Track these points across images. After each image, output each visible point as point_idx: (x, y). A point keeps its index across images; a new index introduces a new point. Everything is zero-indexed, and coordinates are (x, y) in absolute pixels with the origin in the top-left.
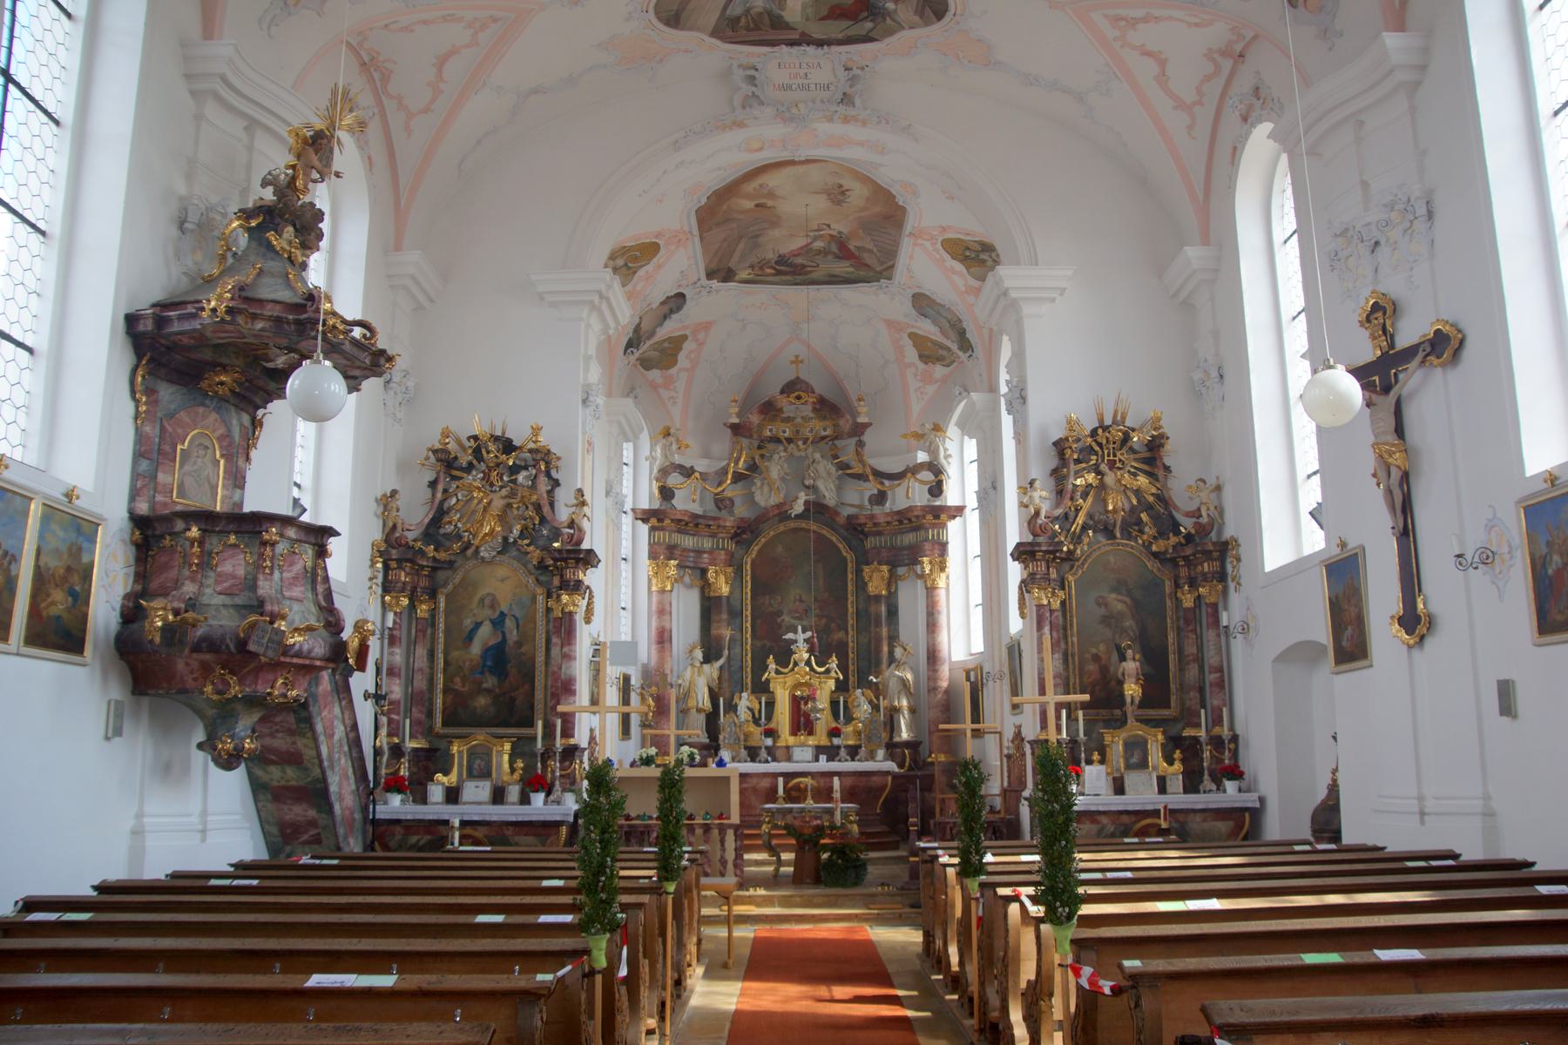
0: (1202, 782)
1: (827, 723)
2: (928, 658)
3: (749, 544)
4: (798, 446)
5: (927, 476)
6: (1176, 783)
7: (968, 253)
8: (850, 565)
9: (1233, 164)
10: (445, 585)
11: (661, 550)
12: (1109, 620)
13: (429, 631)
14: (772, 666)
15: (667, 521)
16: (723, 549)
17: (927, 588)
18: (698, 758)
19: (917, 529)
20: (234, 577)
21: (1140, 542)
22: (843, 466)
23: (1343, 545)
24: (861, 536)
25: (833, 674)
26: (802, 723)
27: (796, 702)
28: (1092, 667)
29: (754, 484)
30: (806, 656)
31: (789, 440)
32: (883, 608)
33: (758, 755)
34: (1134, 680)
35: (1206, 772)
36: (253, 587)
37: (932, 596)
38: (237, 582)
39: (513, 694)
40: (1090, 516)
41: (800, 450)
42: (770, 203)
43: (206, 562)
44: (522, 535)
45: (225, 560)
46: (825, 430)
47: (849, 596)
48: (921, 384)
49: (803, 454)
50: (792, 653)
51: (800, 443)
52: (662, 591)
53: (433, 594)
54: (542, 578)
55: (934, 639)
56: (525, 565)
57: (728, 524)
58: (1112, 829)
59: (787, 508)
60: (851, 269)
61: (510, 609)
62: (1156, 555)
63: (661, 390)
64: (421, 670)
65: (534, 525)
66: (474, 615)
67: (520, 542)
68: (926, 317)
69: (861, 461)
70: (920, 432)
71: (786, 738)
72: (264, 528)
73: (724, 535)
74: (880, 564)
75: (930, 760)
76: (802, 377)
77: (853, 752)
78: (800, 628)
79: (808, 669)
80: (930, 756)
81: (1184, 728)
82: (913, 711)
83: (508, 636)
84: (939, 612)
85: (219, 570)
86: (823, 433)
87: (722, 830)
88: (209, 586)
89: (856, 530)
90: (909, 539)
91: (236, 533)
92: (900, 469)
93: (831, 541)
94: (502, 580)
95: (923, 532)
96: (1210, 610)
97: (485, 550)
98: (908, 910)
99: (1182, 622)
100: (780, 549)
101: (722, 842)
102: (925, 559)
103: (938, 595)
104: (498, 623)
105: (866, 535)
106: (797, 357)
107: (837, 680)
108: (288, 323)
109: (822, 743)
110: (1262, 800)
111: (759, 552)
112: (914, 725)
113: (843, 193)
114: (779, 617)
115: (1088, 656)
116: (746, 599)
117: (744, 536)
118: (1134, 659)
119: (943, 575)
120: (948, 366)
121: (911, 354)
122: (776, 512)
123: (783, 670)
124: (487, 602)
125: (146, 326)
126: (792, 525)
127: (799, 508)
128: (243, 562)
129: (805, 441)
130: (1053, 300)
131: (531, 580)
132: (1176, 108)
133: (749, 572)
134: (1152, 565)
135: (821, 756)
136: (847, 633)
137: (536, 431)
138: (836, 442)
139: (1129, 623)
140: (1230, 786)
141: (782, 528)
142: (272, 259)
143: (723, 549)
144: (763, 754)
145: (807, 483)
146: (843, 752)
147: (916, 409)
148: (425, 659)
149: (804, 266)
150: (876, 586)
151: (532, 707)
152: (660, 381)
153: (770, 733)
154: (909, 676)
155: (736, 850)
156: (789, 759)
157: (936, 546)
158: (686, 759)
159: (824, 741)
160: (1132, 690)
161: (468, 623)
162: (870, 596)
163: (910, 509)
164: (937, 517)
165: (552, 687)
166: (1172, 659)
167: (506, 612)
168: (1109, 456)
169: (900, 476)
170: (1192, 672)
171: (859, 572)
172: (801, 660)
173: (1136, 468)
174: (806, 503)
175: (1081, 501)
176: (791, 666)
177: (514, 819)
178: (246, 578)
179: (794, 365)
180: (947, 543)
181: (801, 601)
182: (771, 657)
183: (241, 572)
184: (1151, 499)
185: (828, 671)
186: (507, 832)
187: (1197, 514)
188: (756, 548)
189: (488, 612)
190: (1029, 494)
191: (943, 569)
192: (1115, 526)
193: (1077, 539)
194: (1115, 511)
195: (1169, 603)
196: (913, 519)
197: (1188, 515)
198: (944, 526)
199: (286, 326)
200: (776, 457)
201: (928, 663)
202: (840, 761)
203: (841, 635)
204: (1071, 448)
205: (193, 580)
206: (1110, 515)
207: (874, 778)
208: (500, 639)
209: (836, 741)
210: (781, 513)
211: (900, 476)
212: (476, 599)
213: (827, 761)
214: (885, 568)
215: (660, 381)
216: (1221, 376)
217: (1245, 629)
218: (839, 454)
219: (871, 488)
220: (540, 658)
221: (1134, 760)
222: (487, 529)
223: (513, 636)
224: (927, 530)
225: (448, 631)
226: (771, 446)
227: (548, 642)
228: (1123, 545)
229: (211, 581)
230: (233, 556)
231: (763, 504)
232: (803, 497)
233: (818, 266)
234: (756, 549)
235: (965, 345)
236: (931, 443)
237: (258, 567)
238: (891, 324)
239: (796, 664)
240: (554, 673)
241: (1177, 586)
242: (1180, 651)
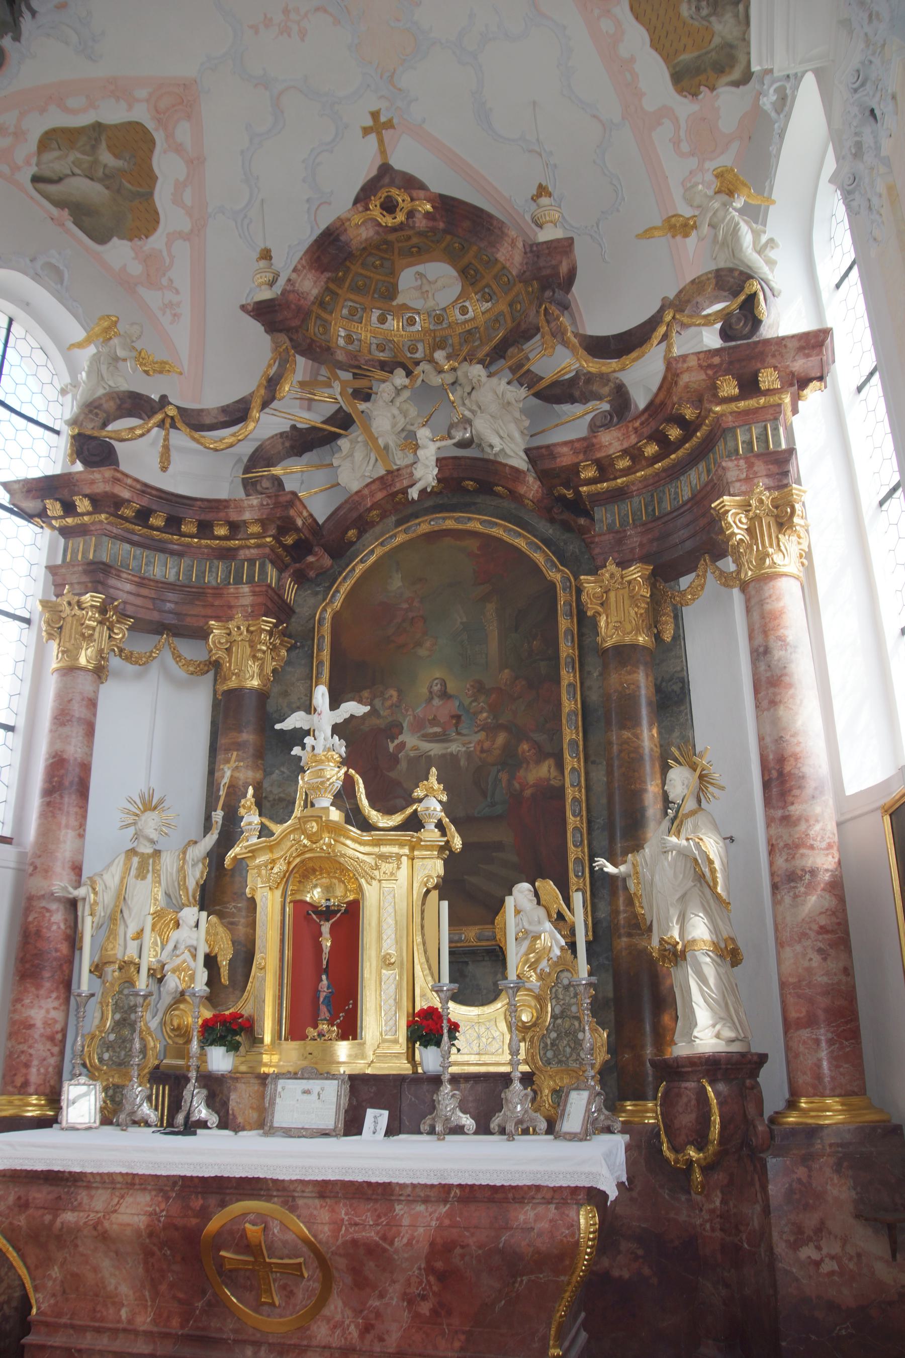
2: (766, 785)
3: (328, 579)
11: (76, 576)
15: (83, 505)
16: (250, 581)
37: (761, 603)
41: (440, 371)
48: (693, 162)
52: (70, 670)
55: (775, 721)
57: (247, 516)
63: (141, 290)
73: (254, 551)
74: (623, 564)
79: (335, 815)
80: (792, 1105)
100: (396, 583)
106: (375, 115)
117: (311, 559)
119: (789, 542)
122: (380, 496)
126: (424, 526)
135: (370, 1113)
143: (250, 581)
152: (136, 269)
154: (712, 846)
157: (760, 467)
179: (373, 138)
180: (791, 451)
181: (445, 695)
185: (414, 823)
188: (345, 587)
196: (689, 413)
201: (768, 802)
202: (432, 1131)
203: (544, 770)
207: (526, 1215)
213: (390, 1132)
215: (136, 269)
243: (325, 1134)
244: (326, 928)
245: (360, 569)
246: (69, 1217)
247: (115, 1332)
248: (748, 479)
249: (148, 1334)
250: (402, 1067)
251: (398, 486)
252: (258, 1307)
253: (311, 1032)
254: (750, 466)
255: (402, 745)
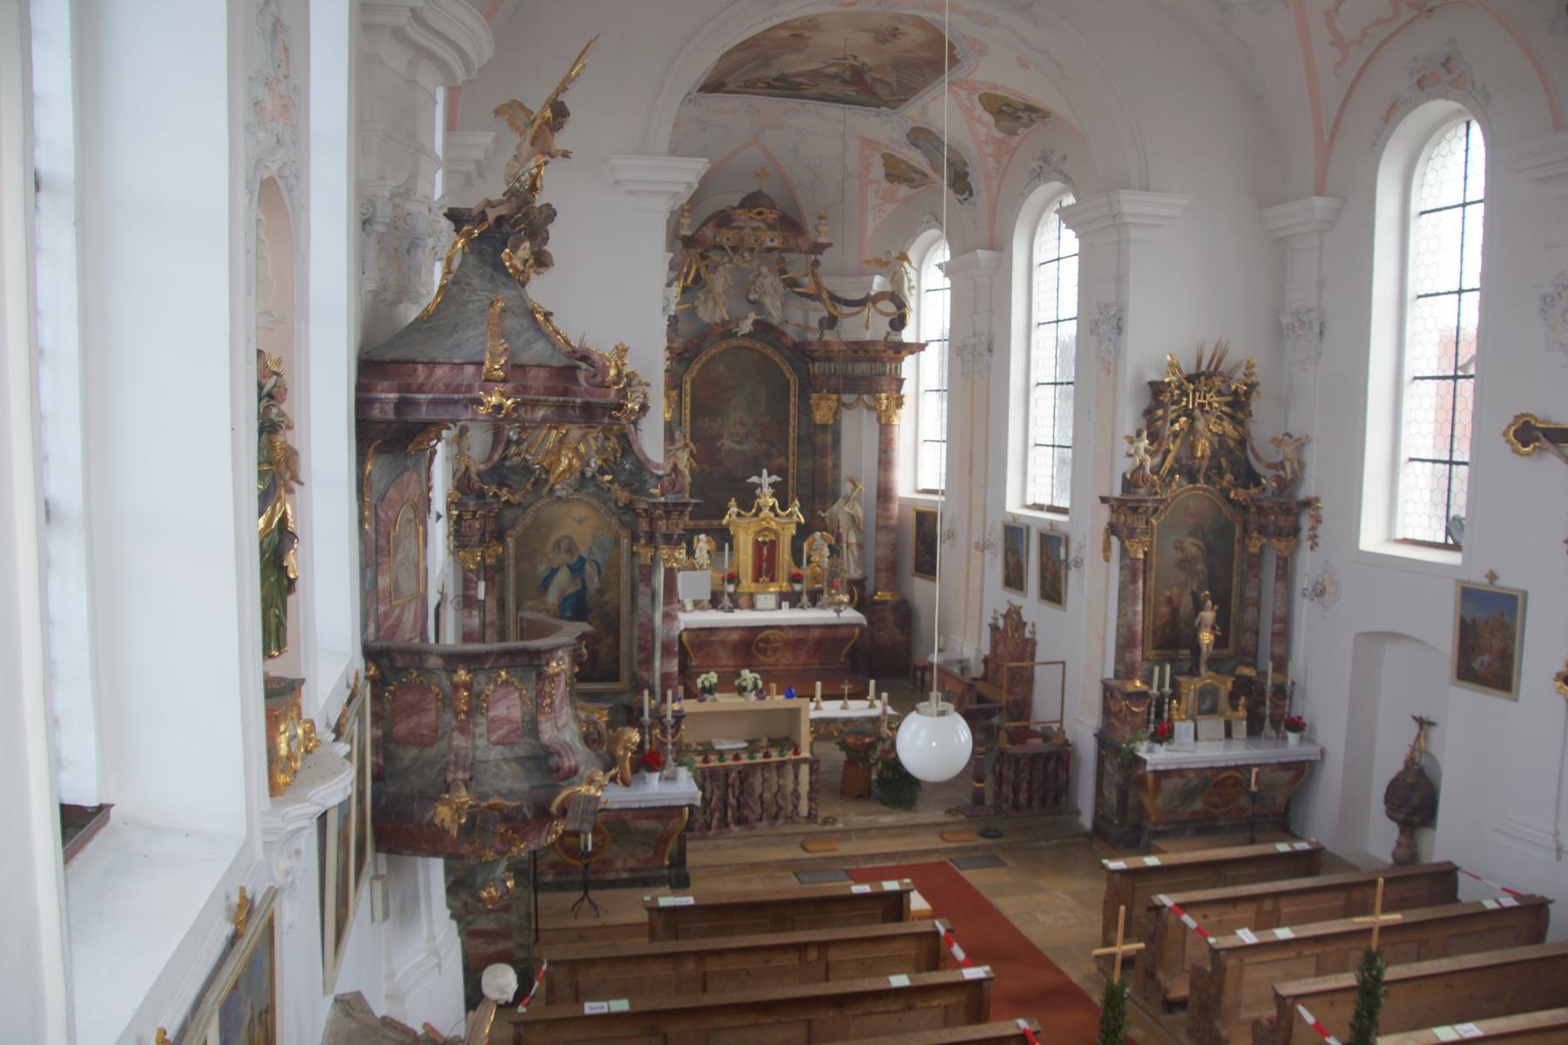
0: (1262, 728)
1: (789, 566)
2: (879, 496)
3: (689, 362)
4: (743, 257)
5: (887, 306)
6: (1241, 728)
7: (1005, 108)
8: (792, 388)
9: (1387, 122)
10: (513, 526)
12: (1184, 564)
13: (497, 578)
14: (734, 509)
17: (881, 425)
18: (760, 683)
19: (874, 359)
20: (509, 721)
21: (1218, 487)
22: (792, 283)
23: (1492, 576)
24: (808, 359)
25: (795, 517)
26: (765, 566)
27: (758, 546)
28: (1164, 610)
29: (698, 298)
30: (771, 501)
31: (734, 249)
32: (829, 438)
33: (720, 602)
34: (1209, 629)
35: (1267, 720)
36: (533, 729)
38: (514, 727)
39: (596, 647)
40: (1177, 459)
42: (807, 34)
43: (477, 704)
44: (602, 471)
45: (496, 702)
46: (772, 240)
47: (791, 421)
49: (748, 266)
50: (756, 497)
51: (747, 255)
53: (500, 537)
54: (626, 518)
56: (605, 503)
58: (1196, 782)
59: (733, 325)
60: (854, 94)
61: (590, 554)
62: (1230, 501)
64: (492, 624)
65: (616, 458)
66: (549, 560)
67: (600, 478)
68: (917, 147)
69: (818, 284)
70: (884, 260)
71: (747, 584)
72: (544, 662)
74: (829, 392)
75: (876, 598)
76: (765, 191)
77: (815, 599)
78: (765, 472)
79: (772, 515)
80: (875, 593)
81: (1236, 667)
82: (860, 546)
83: (589, 584)
84: (892, 449)
85: (491, 714)
86: (769, 244)
87: (796, 764)
88: (481, 736)
89: (802, 353)
90: (862, 368)
91: (508, 668)
92: (858, 295)
93: (775, 362)
94: (581, 521)
95: (879, 365)
96: (1281, 563)
97: (563, 489)
98: (982, 841)
99: (1245, 566)
100: (721, 368)
101: (796, 776)
102: (883, 395)
103: (892, 432)
104: (577, 569)
105: (814, 360)
106: (763, 169)
107: (798, 524)
108: (573, 408)
109: (784, 589)
110: (1323, 752)
111: (700, 370)
112: (861, 563)
113: (894, 35)
114: (719, 440)
115: (1162, 599)
116: (685, 421)
118: (1212, 609)
120: (915, 187)
121: (878, 171)
122: (721, 330)
123: (743, 513)
124: (564, 545)
125: (383, 411)
126: (734, 343)
127: (746, 327)
128: (518, 702)
129: (752, 250)
130: (1160, 226)
131: (614, 521)
132: (1333, 44)
133: (689, 391)
134: (1227, 510)
136: (787, 459)
137: (622, 351)
138: (783, 255)
139: (1200, 567)
140: (1292, 738)
141: (724, 345)
142: (505, 285)
144: (726, 601)
145: (752, 297)
146: (805, 599)
147: (871, 225)
148: (495, 611)
149: (801, 84)
150: (822, 415)
151: (617, 660)
153: (733, 578)
154: (859, 511)
155: (811, 783)
156: (752, 606)
157: (894, 382)
158: (750, 686)
159: (785, 586)
160: (1206, 638)
161: (542, 569)
162: (815, 425)
163: (873, 343)
164: (898, 352)
165: (640, 638)
166: (1234, 600)
167: (585, 556)
168: (1199, 398)
169: (861, 303)
170: (1249, 616)
171: (804, 395)
172: (766, 506)
173: (1222, 411)
174: (756, 323)
175: (1171, 445)
176: (754, 511)
177: (637, 805)
178: (523, 721)
181: (742, 424)
182: (733, 500)
183: (517, 714)
184: (1231, 443)
185: (791, 514)
186: (626, 818)
187: (1281, 465)
189: (564, 557)
190: (1136, 444)
191: (899, 403)
192: (1198, 471)
193: (1166, 484)
194: (1202, 457)
195: (1237, 548)
197: (1270, 466)
198: (902, 359)
199: (570, 411)
200: (721, 268)
202: (802, 607)
203: (781, 460)
204: (1171, 392)
205: (463, 730)
206: (1197, 461)
207: (842, 630)
208: (579, 586)
209: (797, 587)
210: (726, 331)
211: (861, 303)
212: (550, 546)
214: (835, 397)
216: (1321, 332)
217: (1319, 592)
218: (787, 269)
219: (817, 312)
220: (625, 609)
221: (1205, 707)
222: (565, 462)
223: (594, 582)
224: (884, 364)
225: (519, 578)
226: (715, 256)
227: (634, 588)
228: (1204, 490)
229: (482, 729)
230: (504, 697)
231: (706, 319)
232: (753, 316)
233: (817, 85)
234: (695, 368)
235: (961, 182)
236: (895, 273)
237: (539, 707)
238: (865, 142)
239: (760, 509)
240: (641, 625)
241: (1245, 531)
242: (1242, 593)
243: (773, 610)
244: (765, 548)
245: (704, 358)
246: (713, 638)
247: (721, 667)
248: (889, 386)
249: (731, 666)
250: (790, 589)
251: (730, 327)
252: (765, 656)
253: (761, 580)
254: (891, 380)
255: (723, 444)
